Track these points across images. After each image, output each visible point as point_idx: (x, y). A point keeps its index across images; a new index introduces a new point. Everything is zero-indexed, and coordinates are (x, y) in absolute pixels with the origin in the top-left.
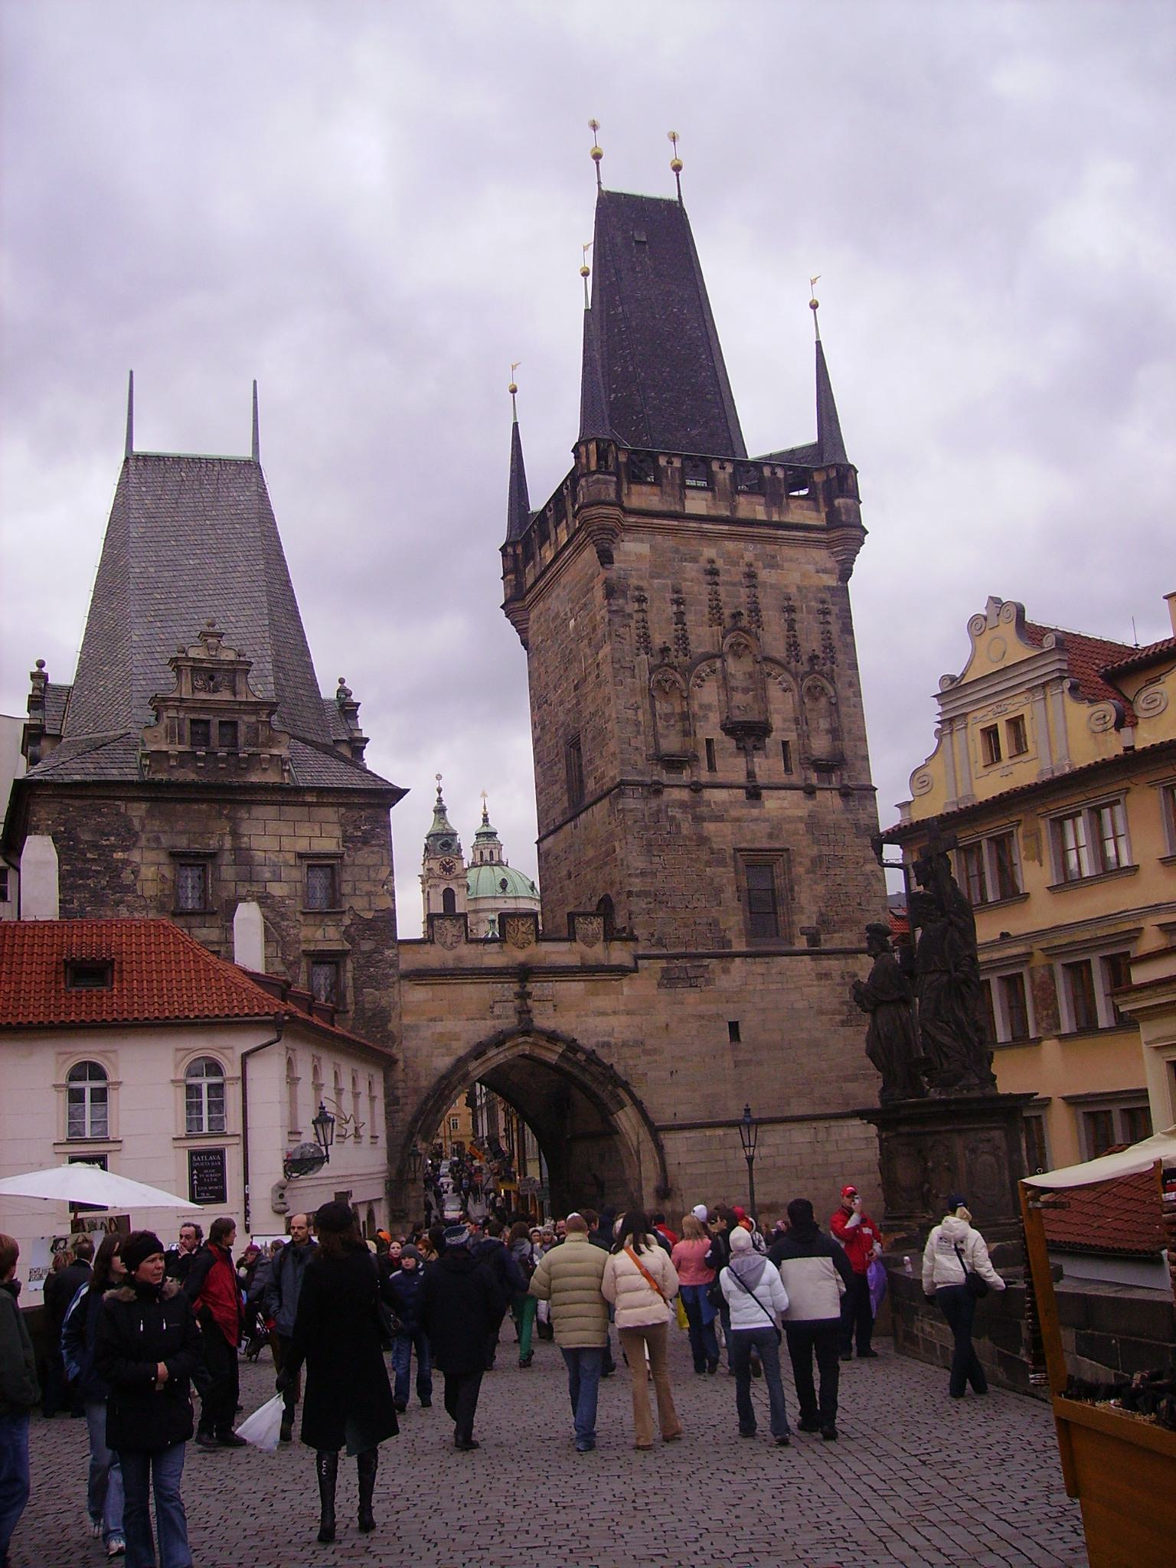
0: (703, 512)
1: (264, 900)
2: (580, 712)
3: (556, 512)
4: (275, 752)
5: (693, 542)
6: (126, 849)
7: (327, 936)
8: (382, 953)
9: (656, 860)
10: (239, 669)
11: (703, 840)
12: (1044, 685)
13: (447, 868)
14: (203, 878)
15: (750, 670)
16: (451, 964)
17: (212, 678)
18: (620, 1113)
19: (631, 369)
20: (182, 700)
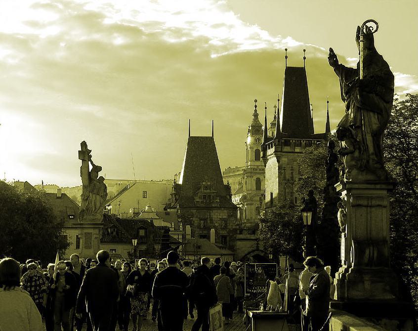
7: (224, 233)
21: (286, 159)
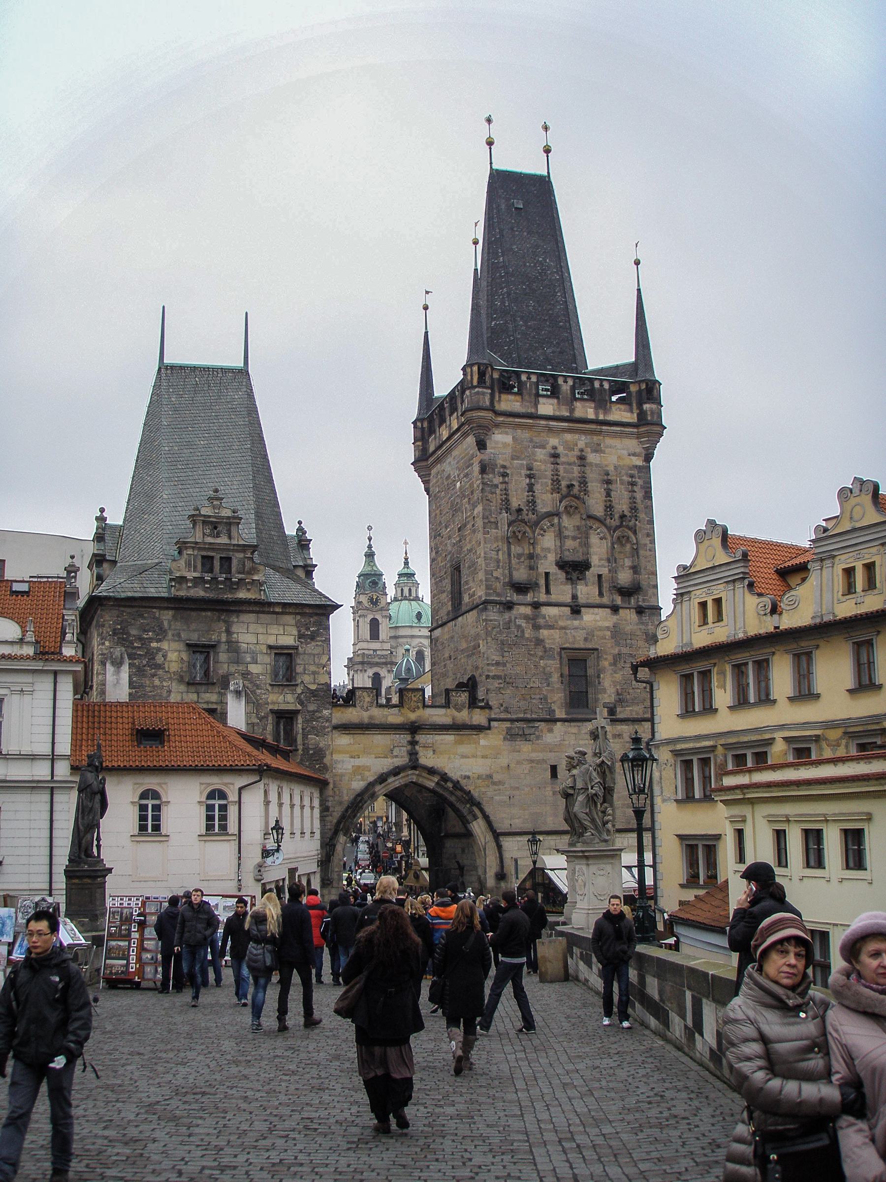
2: (461, 548)
3: (451, 405)
4: (256, 578)
5: (542, 434)
7: (285, 700)
8: (321, 712)
9: (506, 654)
10: (232, 522)
11: (539, 642)
12: (734, 581)
13: (374, 602)
14: (207, 660)
15: (578, 524)
16: (366, 721)
17: (216, 528)
18: (474, 823)
19: (507, 304)
20: (196, 543)
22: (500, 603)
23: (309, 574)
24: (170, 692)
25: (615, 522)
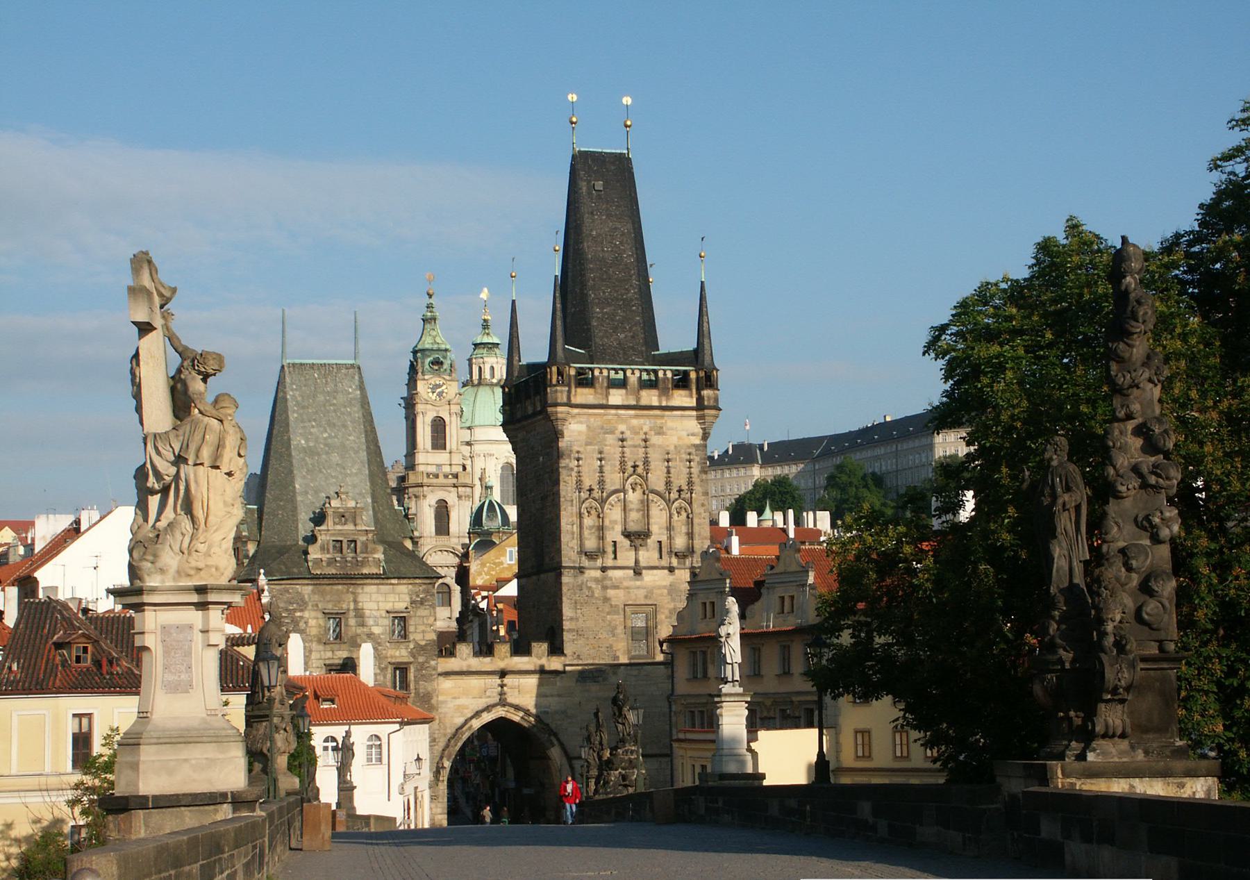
0: (620, 403)
1: (370, 636)
6: (301, 611)
7: (401, 654)
14: (339, 624)
21: (583, 428)
22: (573, 568)
23: (415, 543)
24: (311, 651)
25: (674, 495)
